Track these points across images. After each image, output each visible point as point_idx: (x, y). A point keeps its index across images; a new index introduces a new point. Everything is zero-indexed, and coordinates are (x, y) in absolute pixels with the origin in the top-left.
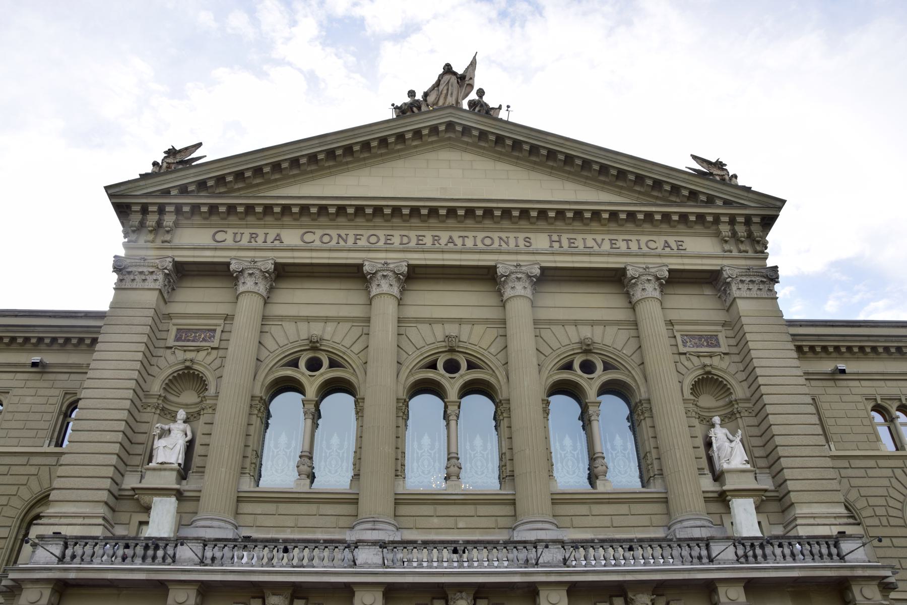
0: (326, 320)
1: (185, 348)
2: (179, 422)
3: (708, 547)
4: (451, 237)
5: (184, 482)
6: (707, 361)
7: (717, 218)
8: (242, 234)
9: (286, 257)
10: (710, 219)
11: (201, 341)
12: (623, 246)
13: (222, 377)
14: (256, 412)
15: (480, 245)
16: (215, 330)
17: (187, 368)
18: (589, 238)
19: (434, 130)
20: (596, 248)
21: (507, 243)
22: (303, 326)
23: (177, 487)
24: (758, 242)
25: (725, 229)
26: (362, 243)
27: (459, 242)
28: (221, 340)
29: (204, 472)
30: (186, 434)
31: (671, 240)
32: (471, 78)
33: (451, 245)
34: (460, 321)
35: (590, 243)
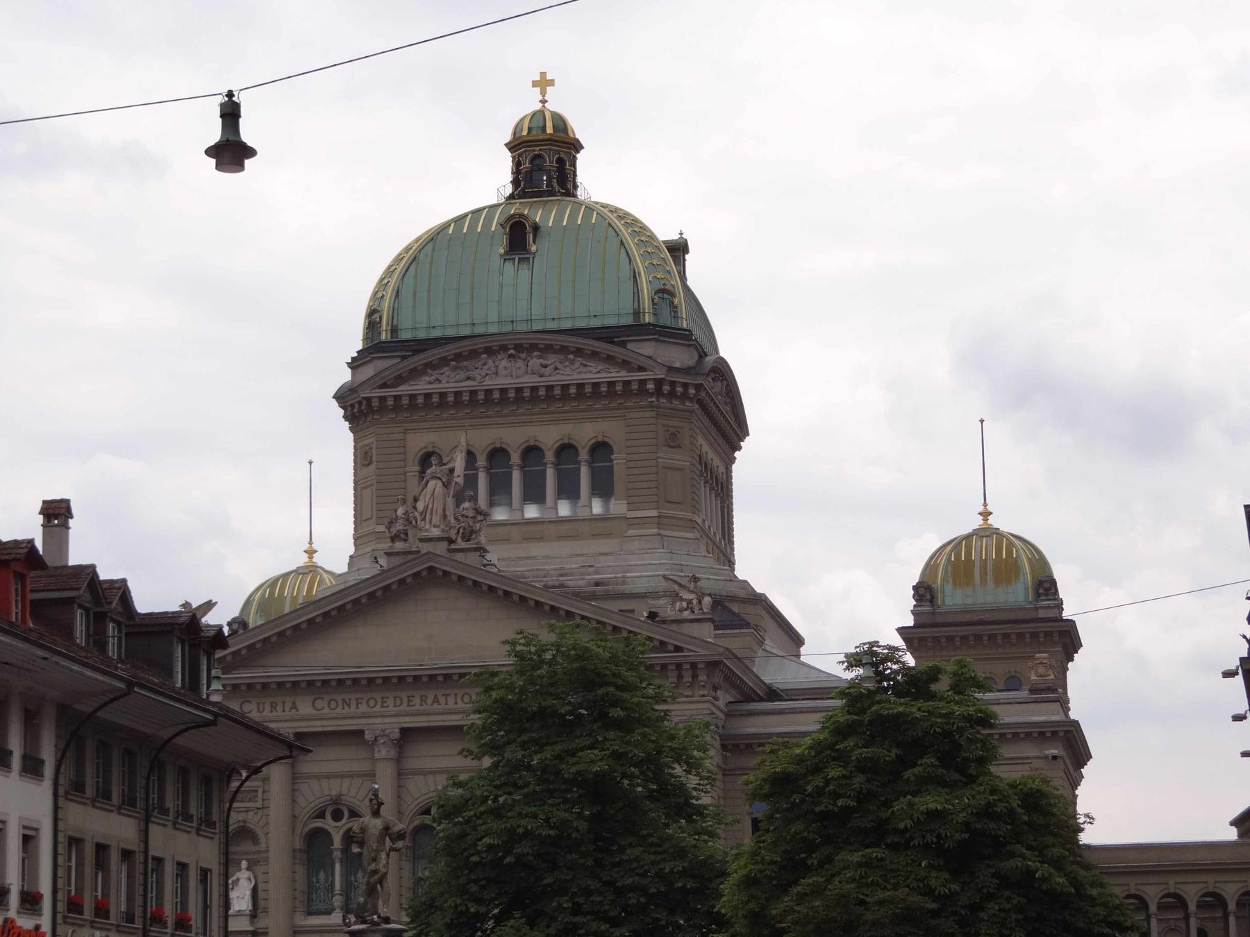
0: (342, 776)
1: (237, 810)
2: (243, 871)
4: (436, 696)
5: (256, 920)
7: (664, 667)
8: (264, 703)
11: (248, 802)
13: (268, 833)
14: (298, 861)
16: (257, 791)
17: (240, 826)
19: (416, 575)
22: (324, 783)
23: (251, 929)
24: (703, 686)
27: (442, 700)
28: (263, 800)
29: (267, 912)
30: (250, 880)
32: (458, 476)
33: (435, 705)
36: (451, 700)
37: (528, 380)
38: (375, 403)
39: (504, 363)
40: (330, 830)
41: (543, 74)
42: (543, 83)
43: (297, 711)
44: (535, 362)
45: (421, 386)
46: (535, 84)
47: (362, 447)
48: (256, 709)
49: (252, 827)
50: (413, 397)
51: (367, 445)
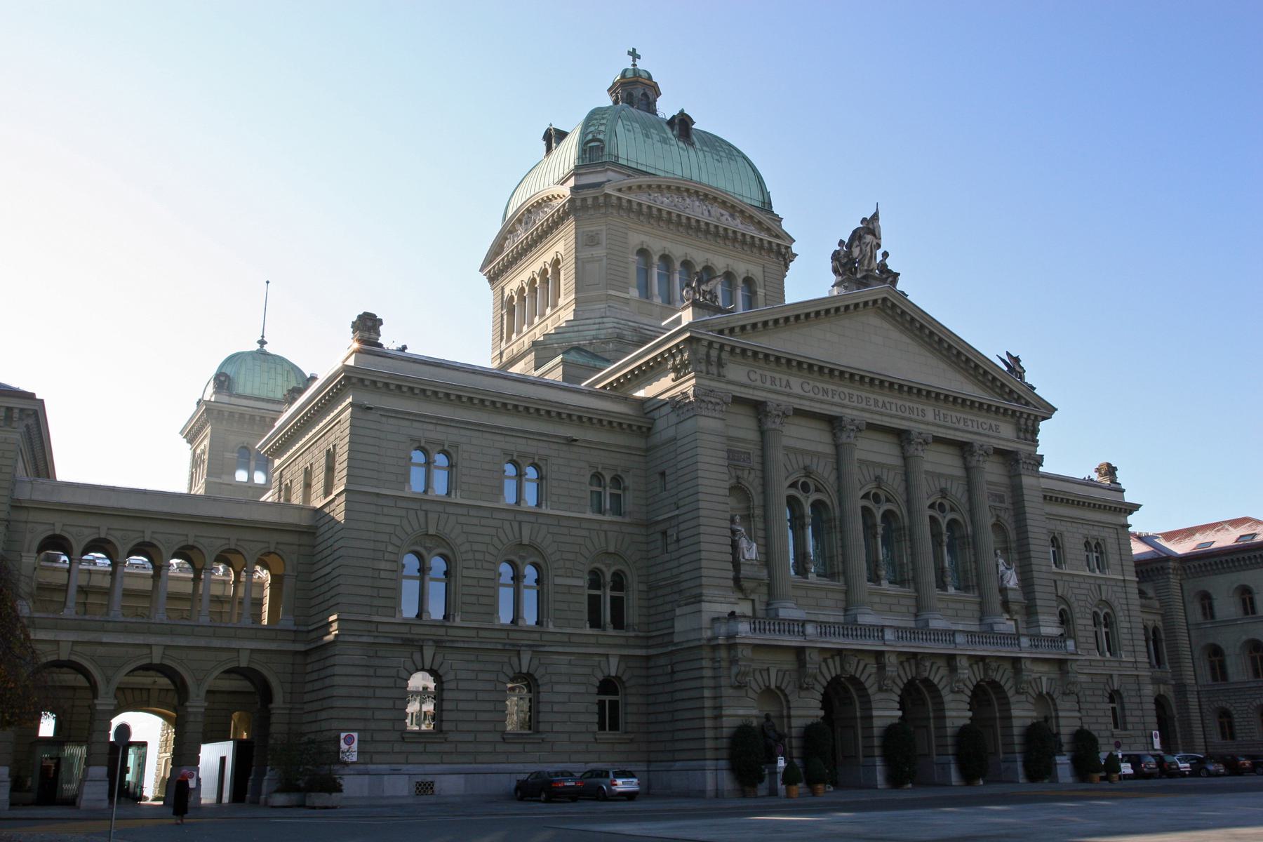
3: (1018, 639)
6: (998, 512)
9: (798, 404)
10: (1018, 414)
12: (970, 423)
15: (900, 413)
18: (954, 414)
19: (875, 302)
20: (956, 426)
21: (913, 412)
25: (1022, 421)
26: (836, 399)
27: (888, 405)
31: (994, 423)
34: (882, 465)
35: (954, 420)
36: (894, 407)
37: (713, 221)
38: (614, 201)
39: (697, 203)
40: (802, 499)
41: (634, 50)
42: (634, 54)
43: (790, 388)
44: (716, 210)
45: (644, 199)
46: (629, 53)
47: (583, 232)
48: (759, 378)
49: (747, 485)
50: (640, 205)
51: (592, 231)
